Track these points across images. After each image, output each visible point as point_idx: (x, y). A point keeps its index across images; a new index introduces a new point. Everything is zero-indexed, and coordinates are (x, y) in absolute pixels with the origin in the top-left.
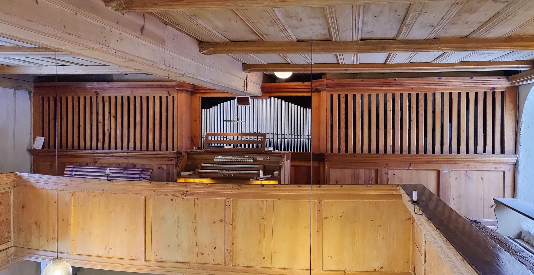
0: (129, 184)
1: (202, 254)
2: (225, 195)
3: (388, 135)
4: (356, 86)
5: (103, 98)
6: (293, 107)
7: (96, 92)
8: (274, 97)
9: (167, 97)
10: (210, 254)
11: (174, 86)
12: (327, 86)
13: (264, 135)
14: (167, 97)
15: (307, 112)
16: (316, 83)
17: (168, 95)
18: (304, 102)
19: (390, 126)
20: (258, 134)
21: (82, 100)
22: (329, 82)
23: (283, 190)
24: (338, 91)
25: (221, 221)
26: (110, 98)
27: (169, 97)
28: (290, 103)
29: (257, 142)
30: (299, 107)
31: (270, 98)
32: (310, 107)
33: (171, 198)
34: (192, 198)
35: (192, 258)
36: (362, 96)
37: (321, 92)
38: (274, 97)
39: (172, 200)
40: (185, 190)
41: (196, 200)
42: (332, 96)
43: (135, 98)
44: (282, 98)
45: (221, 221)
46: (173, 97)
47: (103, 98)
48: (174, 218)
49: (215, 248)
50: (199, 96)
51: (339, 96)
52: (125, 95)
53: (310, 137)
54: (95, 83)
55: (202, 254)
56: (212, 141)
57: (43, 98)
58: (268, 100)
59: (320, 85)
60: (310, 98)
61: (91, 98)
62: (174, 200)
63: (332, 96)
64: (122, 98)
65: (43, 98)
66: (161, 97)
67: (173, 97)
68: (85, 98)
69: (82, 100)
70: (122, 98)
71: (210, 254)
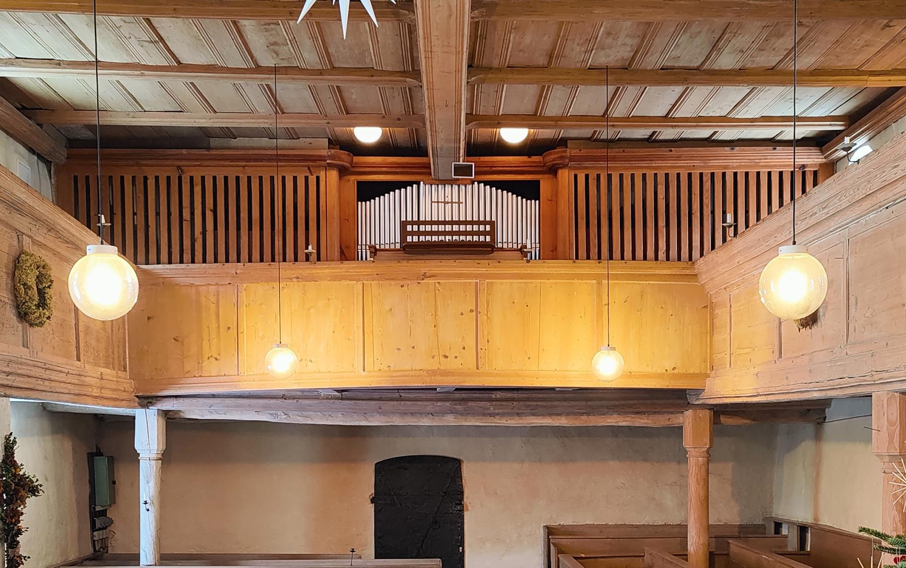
0: (342, 266)
1: (446, 357)
2: (476, 276)
3: (660, 235)
4: (614, 159)
5: (192, 178)
6: (510, 198)
7: (179, 167)
8: (479, 182)
9: (307, 178)
10: (456, 357)
11: (324, 156)
12: (572, 159)
13: (492, 224)
14: (307, 178)
15: (533, 205)
16: (552, 157)
17: (308, 174)
18: (528, 191)
19: (662, 223)
20: (485, 223)
21: (151, 183)
22: (575, 152)
23: (553, 267)
24: (586, 168)
25: (472, 311)
26: (203, 178)
27: (310, 177)
28: (505, 192)
29: (485, 233)
30: (519, 198)
31: (473, 183)
32: (537, 197)
33: (402, 283)
34: (431, 281)
35: (433, 365)
36: (621, 176)
37: (560, 172)
38: (479, 182)
39: (402, 286)
40: (423, 271)
41: (437, 285)
42: (576, 176)
43: (249, 178)
44: (492, 184)
45: (472, 311)
46: (318, 178)
47: (192, 178)
48: (406, 311)
49: (464, 348)
50: (354, 178)
51: (587, 176)
52: (232, 174)
53: (538, 245)
54: (184, 151)
55: (446, 357)
56: (412, 233)
57: (76, 178)
58: (469, 187)
59: (562, 157)
60: (537, 183)
61: (168, 178)
62: (405, 288)
63: (576, 176)
64: (226, 178)
65: (76, 178)
66: (295, 178)
67: (318, 178)
68: (157, 178)
69: (151, 183)
70: (226, 178)
71: (456, 357)
